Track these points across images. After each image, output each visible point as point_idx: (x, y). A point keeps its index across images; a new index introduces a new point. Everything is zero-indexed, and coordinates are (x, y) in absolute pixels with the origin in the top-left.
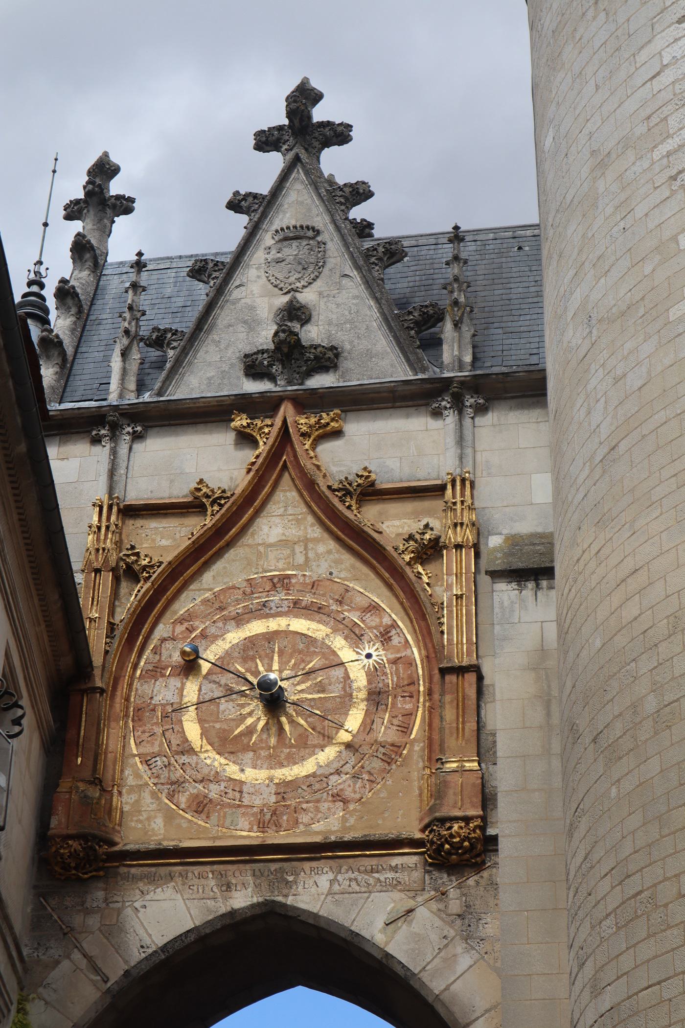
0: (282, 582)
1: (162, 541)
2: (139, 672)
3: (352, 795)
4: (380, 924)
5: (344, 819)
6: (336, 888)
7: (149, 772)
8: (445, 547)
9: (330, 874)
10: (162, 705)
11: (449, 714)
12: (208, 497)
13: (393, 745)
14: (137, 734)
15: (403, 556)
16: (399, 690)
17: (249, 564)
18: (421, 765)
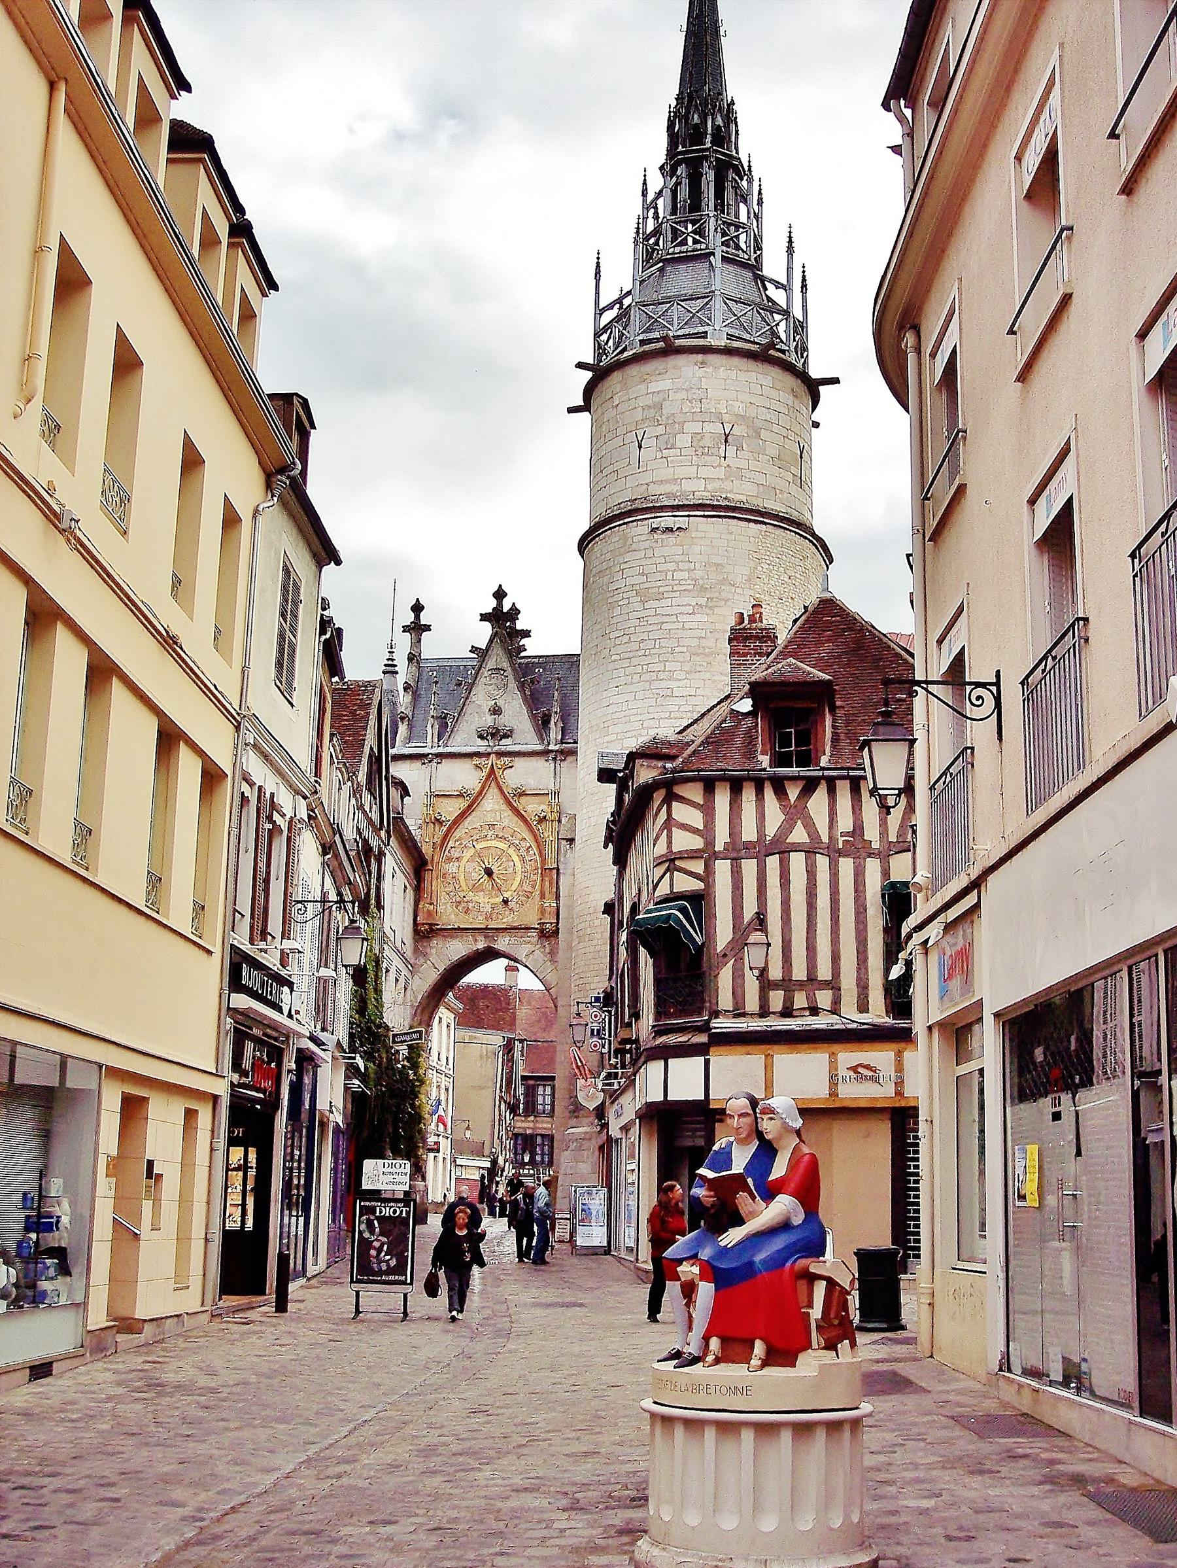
1: (450, 810)
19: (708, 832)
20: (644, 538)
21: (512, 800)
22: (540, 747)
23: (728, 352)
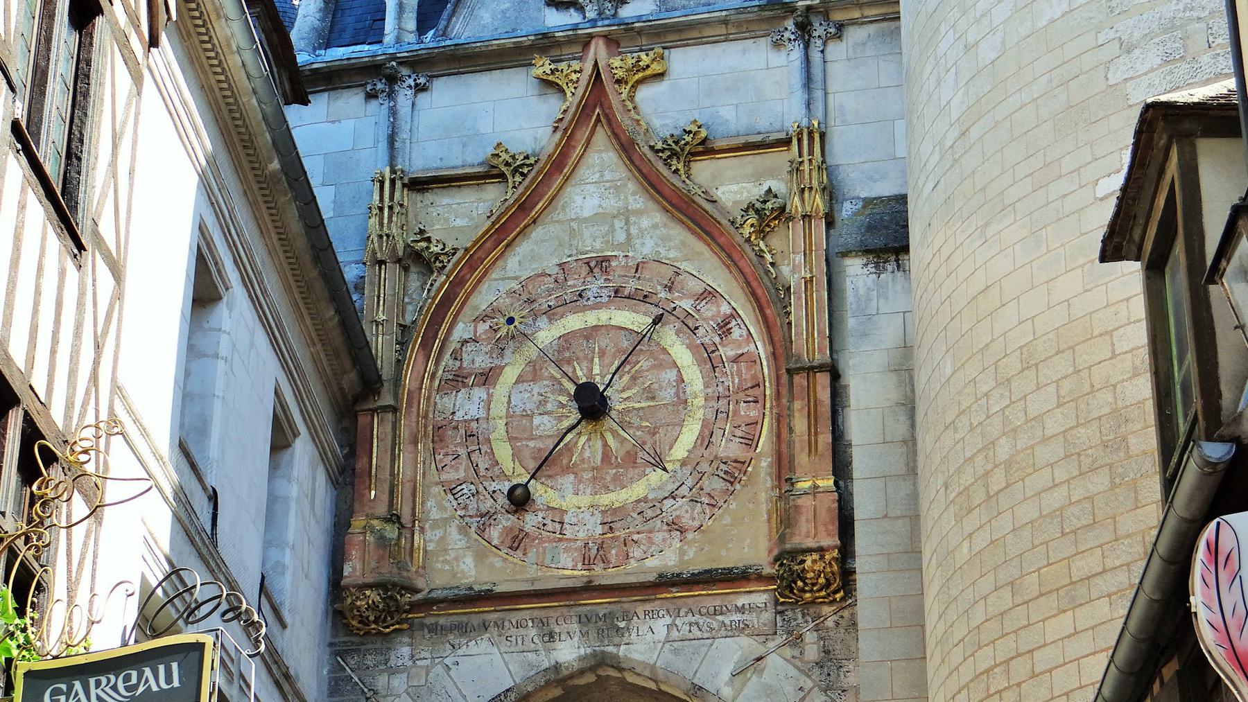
0: (601, 264)
2: (437, 382)
3: (690, 522)
4: (726, 674)
5: (682, 552)
6: (675, 634)
7: (455, 503)
8: (791, 218)
9: (667, 617)
10: (465, 421)
11: (800, 424)
12: (507, 164)
13: (736, 461)
14: (438, 457)
15: (741, 230)
16: (742, 395)
17: (560, 245)
18: (769, 484)
21: (668, 169)
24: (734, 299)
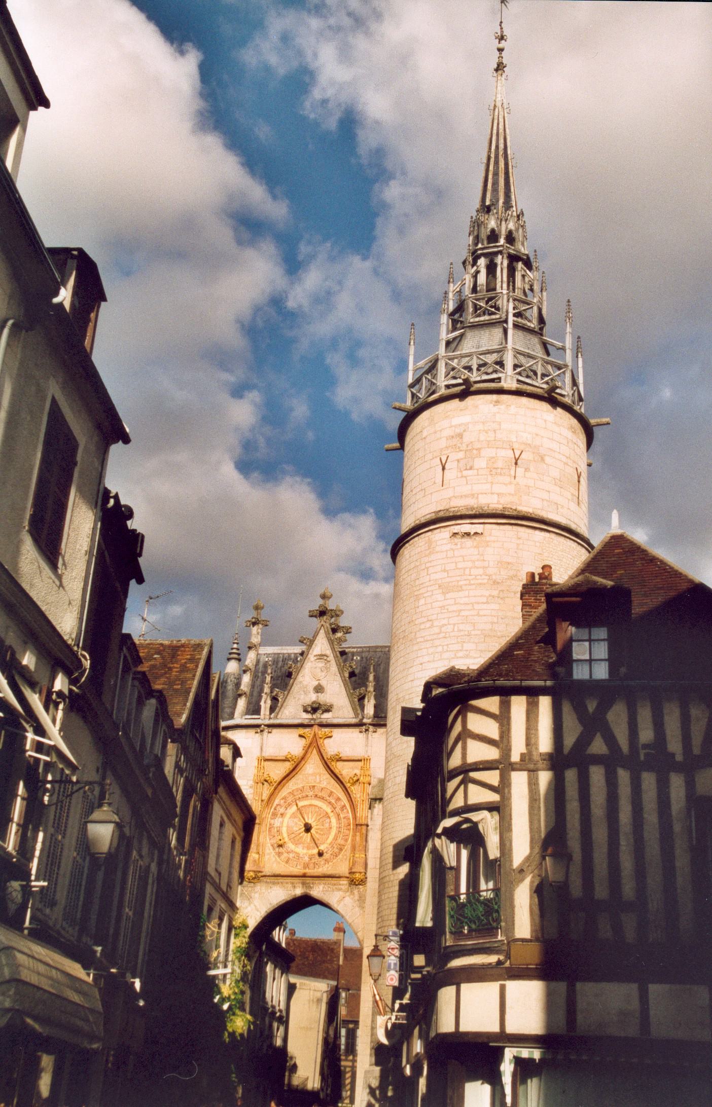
1: (277, 771)
4: (335, 901)
19: (503, 742)
20: (445, 541)
22: (354, 721)
23: (518, 393)
24: (344, 800)
